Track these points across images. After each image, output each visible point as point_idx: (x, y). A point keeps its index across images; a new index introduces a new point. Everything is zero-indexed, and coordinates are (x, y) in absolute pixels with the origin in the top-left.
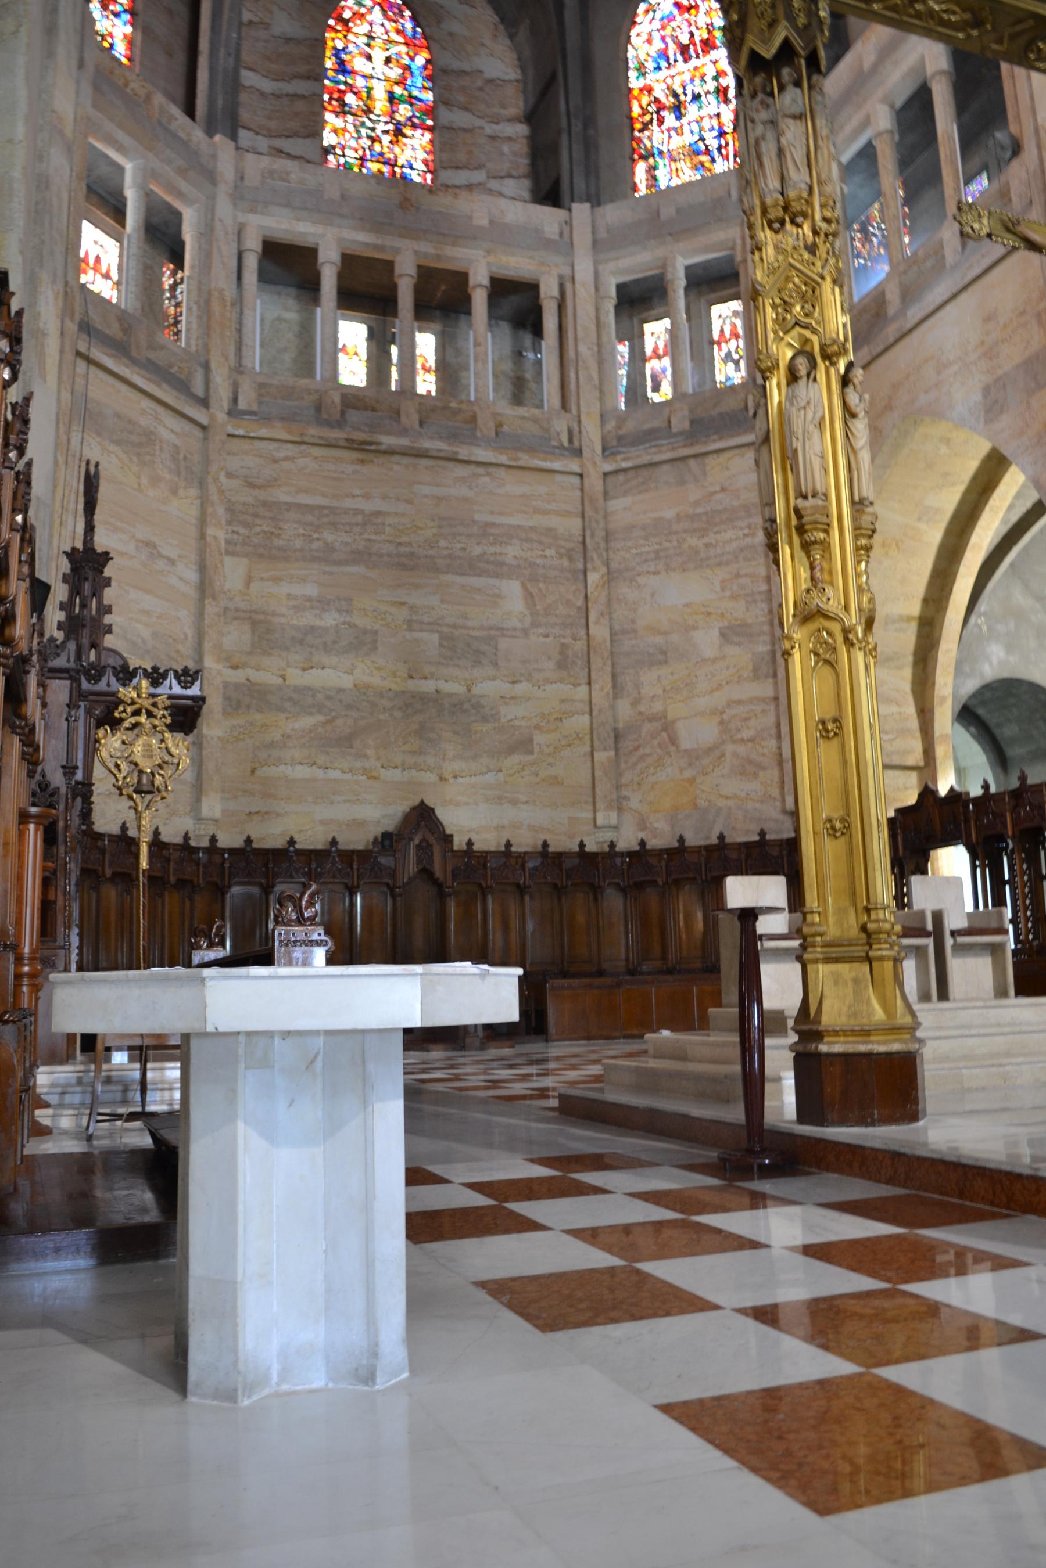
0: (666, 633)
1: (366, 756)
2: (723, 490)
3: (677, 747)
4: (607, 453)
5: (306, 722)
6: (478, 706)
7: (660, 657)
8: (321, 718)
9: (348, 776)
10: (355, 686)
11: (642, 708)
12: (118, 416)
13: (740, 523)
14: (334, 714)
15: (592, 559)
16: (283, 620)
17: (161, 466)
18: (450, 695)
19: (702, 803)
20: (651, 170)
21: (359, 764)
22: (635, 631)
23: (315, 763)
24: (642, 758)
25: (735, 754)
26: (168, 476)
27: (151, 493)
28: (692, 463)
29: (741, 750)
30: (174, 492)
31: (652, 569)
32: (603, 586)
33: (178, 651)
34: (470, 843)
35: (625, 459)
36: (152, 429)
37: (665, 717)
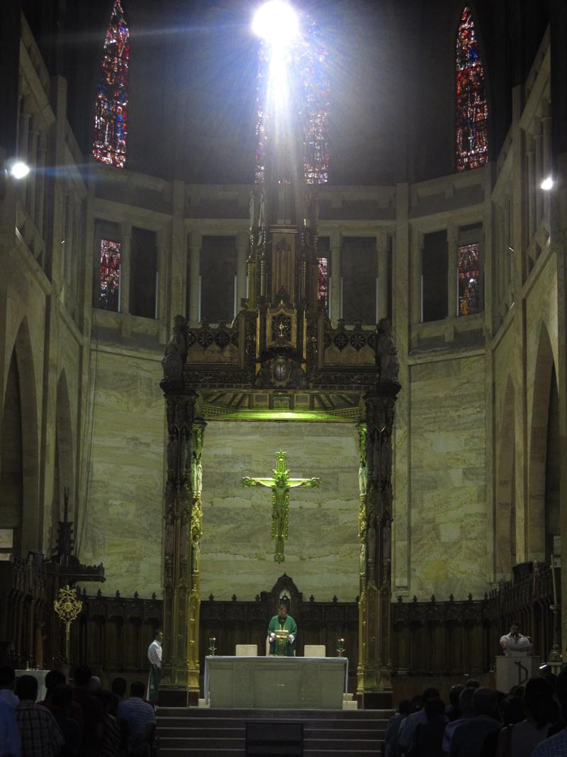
0: (437, 470)
1: (258, 547)
2: (468, 382)
3: (440, 540)
4: (411, 353)
5: (225, 528)
6: (325, 515)
7: (433, 484)
8: (233, 526)
9: (248, 559)
10: (252, 506)
11: (424, 515)
12: (116, 374)
13: (477, 404)
14: (240, 523)
15: (399, 421)
16: (212, 470)
17: (141, 393)
18: (308, 509)
19: (450, 576)
20: (466, 135)
21: (254, 552)
22: (422, 467)
23: (228, 552)
24: (423, 545)
25: (467, 547)
26: (145, 397)
27: (135, 410)
28: (454, 362)
29: (470, 544)
30: (149, 405)
31: (431, 429)
32: (405, 438)
33: (152, 494)
34: (312, 598)
35: (419, 358)
36: (135, 374)
37: (435, 522)
